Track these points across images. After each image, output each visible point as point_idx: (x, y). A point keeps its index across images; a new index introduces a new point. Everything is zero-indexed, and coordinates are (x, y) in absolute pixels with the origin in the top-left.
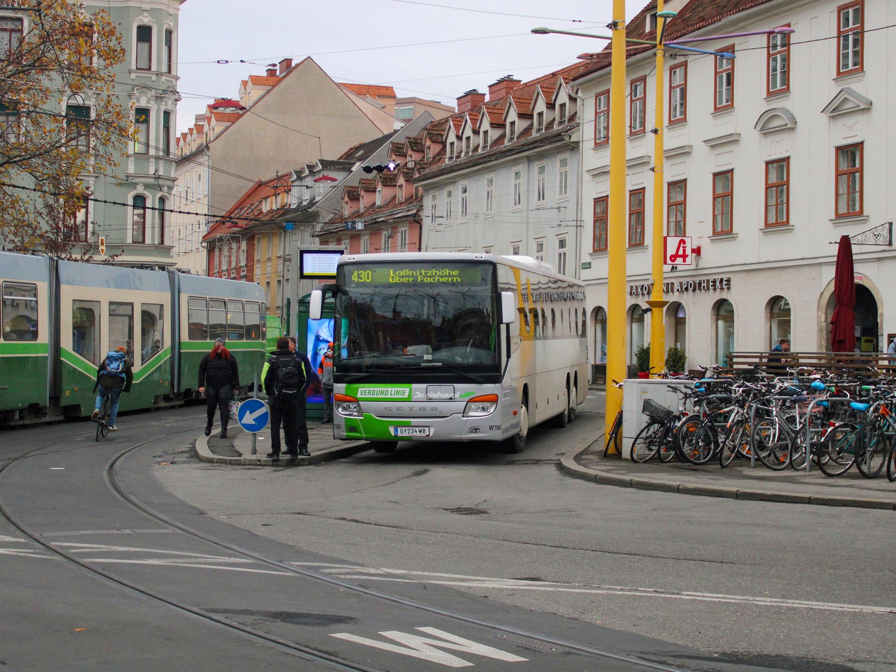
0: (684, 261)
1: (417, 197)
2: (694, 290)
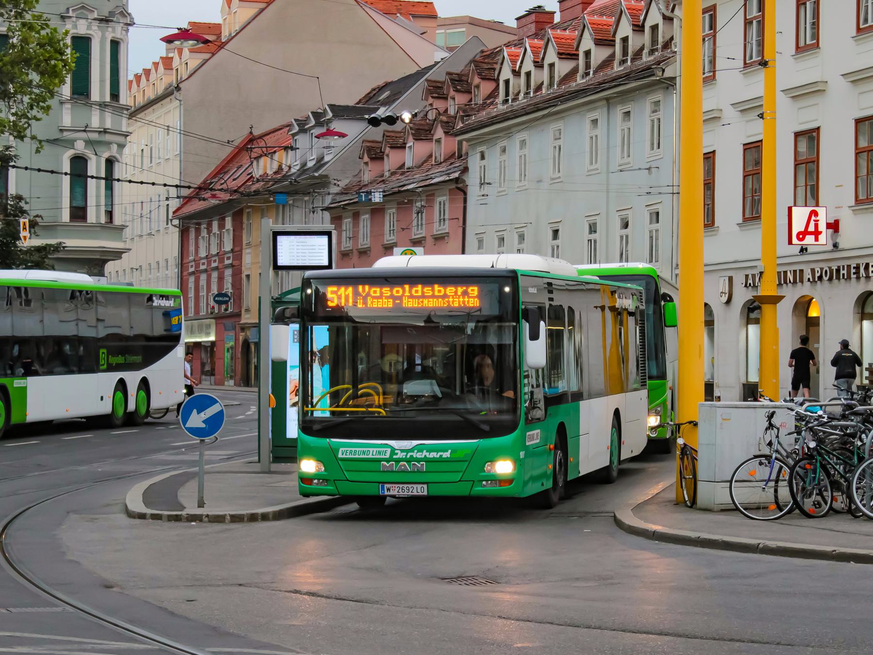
0: (817, 240)
1: (460, 156)
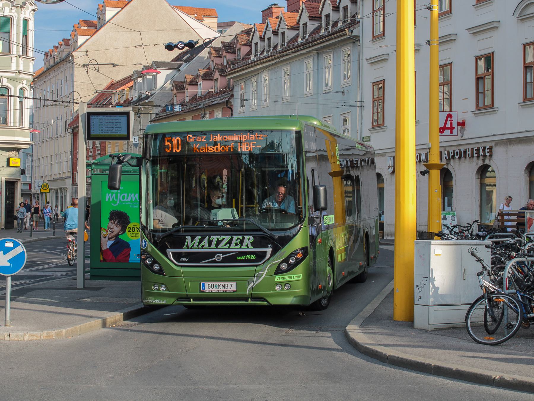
0: (451, 132)
2: (460, 157)
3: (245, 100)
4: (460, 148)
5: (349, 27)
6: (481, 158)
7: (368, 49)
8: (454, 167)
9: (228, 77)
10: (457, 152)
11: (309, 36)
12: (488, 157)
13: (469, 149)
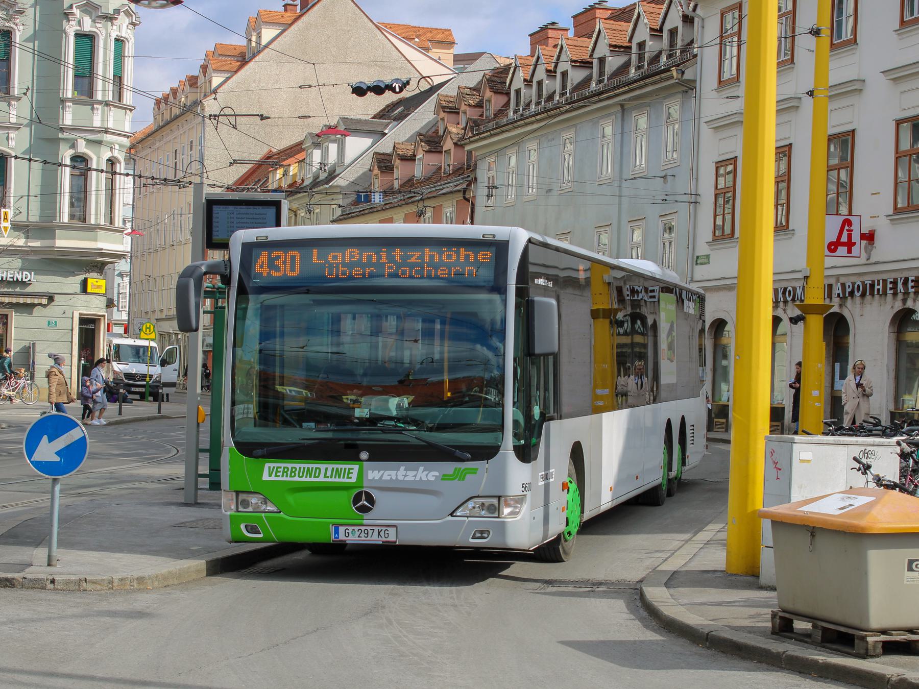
0: (849, 251)
1: (469, 167)
2: (863, 295)
3: (494, 187)
4: (862, 279)
5: (678, 65)
6: (900, 296)
7: (712, 104)
8: (852, 311)
9: (467, 148)
10: (858, 286)
11: (609, 79)
12: (912, 295)
13: (879, 281)
